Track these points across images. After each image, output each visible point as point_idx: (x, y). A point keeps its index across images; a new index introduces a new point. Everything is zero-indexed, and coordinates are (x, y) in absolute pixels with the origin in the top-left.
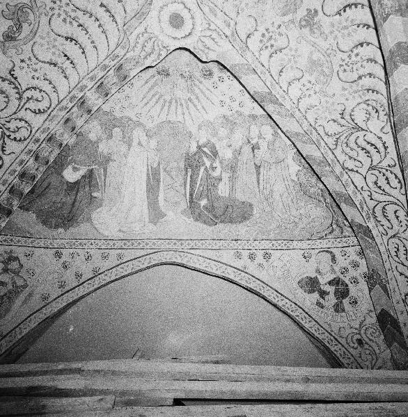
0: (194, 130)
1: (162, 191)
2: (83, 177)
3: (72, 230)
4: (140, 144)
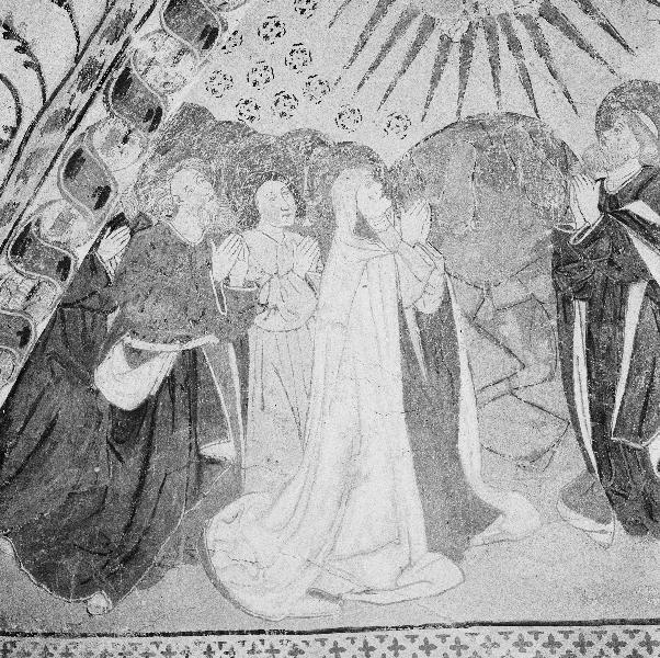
0: (577, 133)
1: (473, 410)
2: (169, 382)
3: (141, 601)
4: (363, 229)
